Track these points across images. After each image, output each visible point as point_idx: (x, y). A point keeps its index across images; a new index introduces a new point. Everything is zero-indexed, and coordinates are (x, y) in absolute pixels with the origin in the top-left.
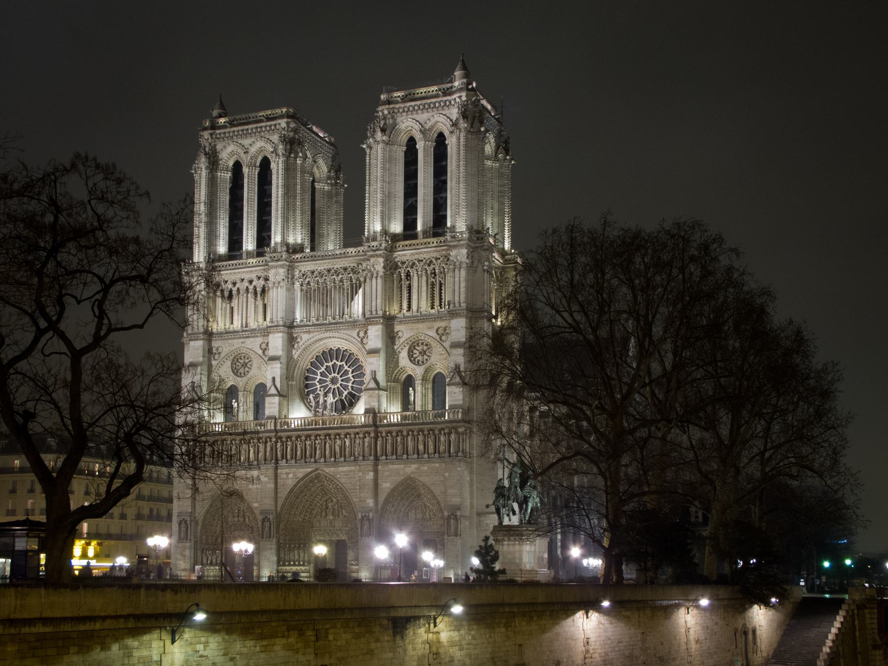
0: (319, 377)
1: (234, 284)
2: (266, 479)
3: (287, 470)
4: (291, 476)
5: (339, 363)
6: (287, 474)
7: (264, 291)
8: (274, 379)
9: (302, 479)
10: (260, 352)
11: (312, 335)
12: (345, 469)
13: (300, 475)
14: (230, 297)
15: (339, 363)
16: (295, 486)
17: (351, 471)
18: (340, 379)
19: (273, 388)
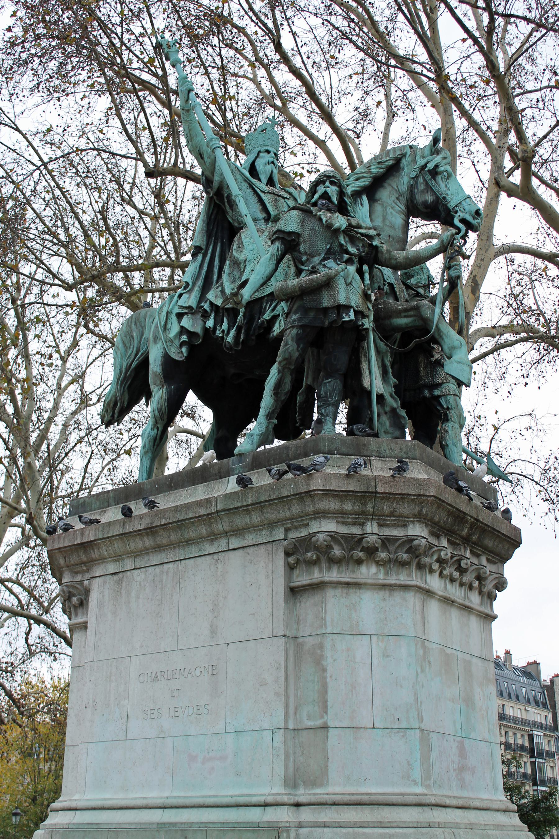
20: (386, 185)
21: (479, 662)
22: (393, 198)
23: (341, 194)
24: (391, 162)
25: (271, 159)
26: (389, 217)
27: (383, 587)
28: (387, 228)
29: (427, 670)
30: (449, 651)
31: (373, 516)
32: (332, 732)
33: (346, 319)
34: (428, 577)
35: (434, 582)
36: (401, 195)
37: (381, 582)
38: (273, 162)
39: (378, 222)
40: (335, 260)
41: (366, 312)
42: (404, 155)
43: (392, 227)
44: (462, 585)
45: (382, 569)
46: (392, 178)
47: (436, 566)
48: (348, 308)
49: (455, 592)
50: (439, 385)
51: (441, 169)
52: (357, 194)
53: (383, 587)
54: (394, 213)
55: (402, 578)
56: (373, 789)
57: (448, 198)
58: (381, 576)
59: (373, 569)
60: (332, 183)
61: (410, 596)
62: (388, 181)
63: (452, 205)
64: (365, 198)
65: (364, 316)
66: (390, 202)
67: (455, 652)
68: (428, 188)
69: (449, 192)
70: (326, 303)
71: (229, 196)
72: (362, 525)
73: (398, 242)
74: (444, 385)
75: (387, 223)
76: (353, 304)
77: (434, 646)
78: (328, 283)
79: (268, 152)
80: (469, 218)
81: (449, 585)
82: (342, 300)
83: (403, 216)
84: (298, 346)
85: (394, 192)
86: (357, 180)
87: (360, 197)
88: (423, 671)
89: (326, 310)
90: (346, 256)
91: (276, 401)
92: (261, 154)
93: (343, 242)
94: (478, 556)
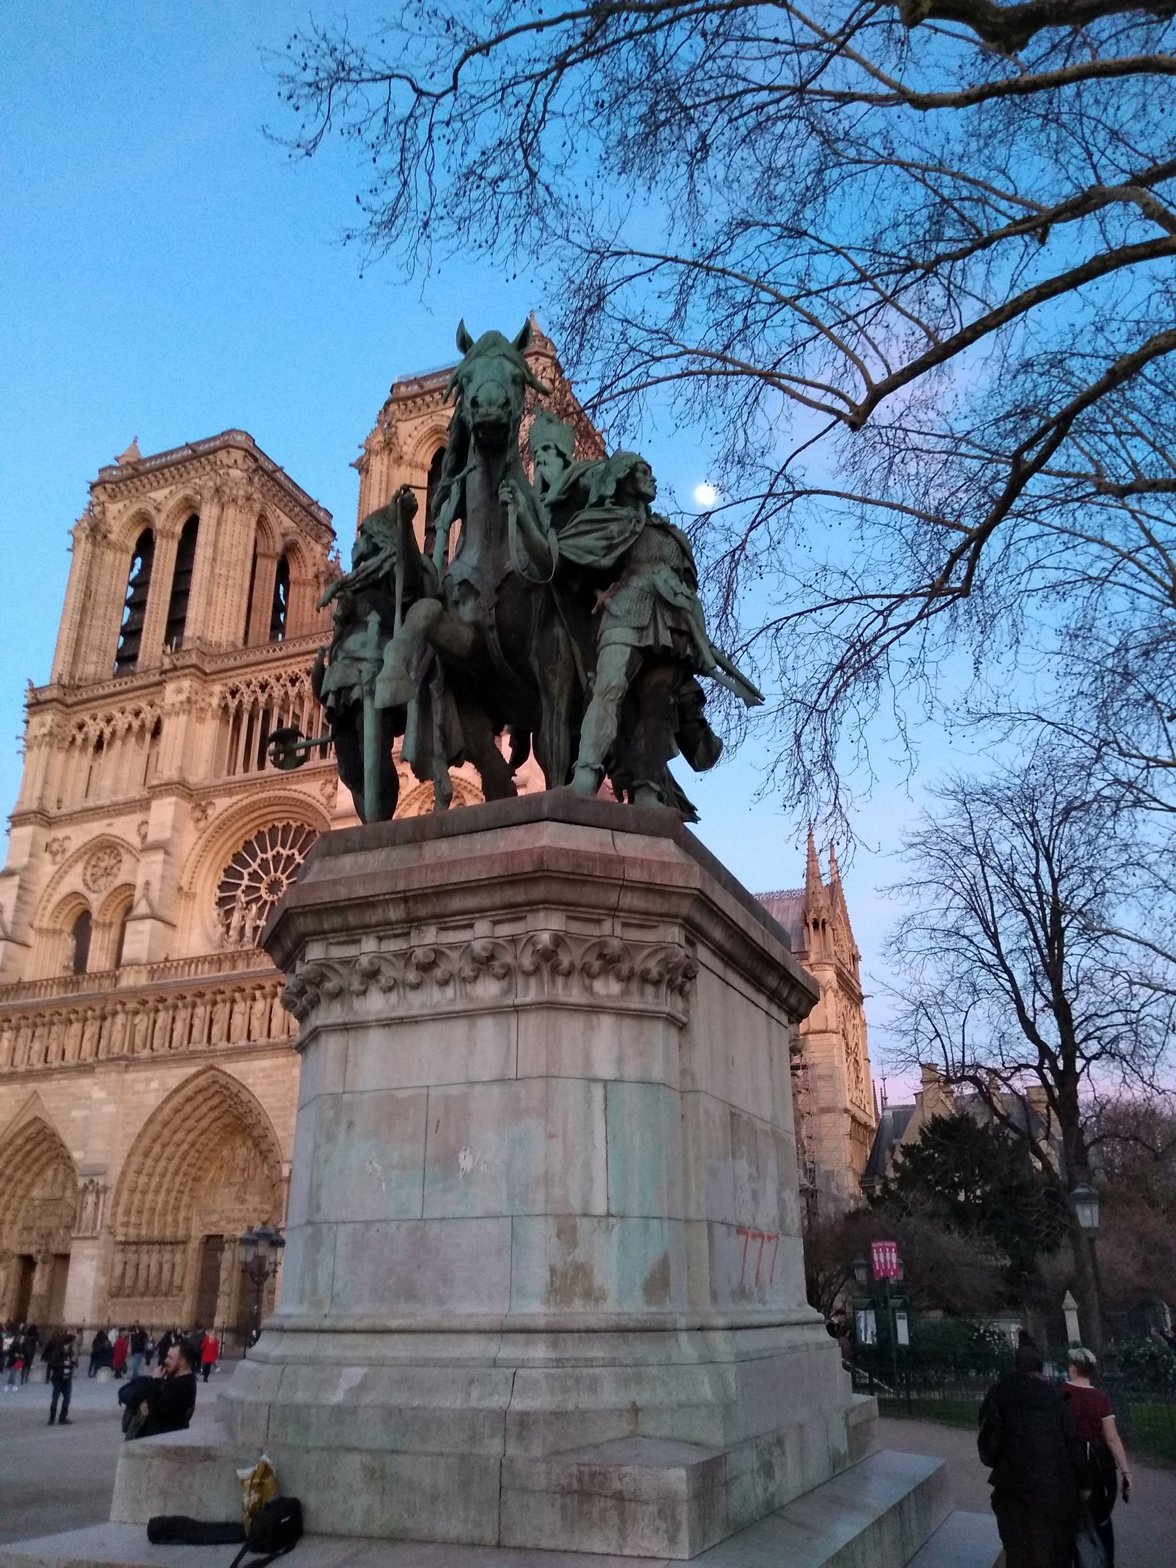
0: (245, 882)
1: (109, 721)
2: (103, 1094)
3: (149, 1074)
4: (154, 1085)
5: (285, 852)
6: (148, 1080)
7: (157, 731)
8: (147, 883)
9: (177, 1090)
10: (136, 841)
11: (235, 798)
12: (266, 1063)
13: (173, 1083)
14: (99, 746)
15: (285, 852)
16: (160, 1109)
17: (277, 1068)
18: (283, 877)
19: (143, 903)
21: (496, 1090)
29: (341, 1136)
30: (399, 1094)
34: (357, 1003)
35: (375, 1004)
41: (354, 680)
44: (444, 983)
65: (351, 688)
67: (424, 1091)
77: (366, 1096)
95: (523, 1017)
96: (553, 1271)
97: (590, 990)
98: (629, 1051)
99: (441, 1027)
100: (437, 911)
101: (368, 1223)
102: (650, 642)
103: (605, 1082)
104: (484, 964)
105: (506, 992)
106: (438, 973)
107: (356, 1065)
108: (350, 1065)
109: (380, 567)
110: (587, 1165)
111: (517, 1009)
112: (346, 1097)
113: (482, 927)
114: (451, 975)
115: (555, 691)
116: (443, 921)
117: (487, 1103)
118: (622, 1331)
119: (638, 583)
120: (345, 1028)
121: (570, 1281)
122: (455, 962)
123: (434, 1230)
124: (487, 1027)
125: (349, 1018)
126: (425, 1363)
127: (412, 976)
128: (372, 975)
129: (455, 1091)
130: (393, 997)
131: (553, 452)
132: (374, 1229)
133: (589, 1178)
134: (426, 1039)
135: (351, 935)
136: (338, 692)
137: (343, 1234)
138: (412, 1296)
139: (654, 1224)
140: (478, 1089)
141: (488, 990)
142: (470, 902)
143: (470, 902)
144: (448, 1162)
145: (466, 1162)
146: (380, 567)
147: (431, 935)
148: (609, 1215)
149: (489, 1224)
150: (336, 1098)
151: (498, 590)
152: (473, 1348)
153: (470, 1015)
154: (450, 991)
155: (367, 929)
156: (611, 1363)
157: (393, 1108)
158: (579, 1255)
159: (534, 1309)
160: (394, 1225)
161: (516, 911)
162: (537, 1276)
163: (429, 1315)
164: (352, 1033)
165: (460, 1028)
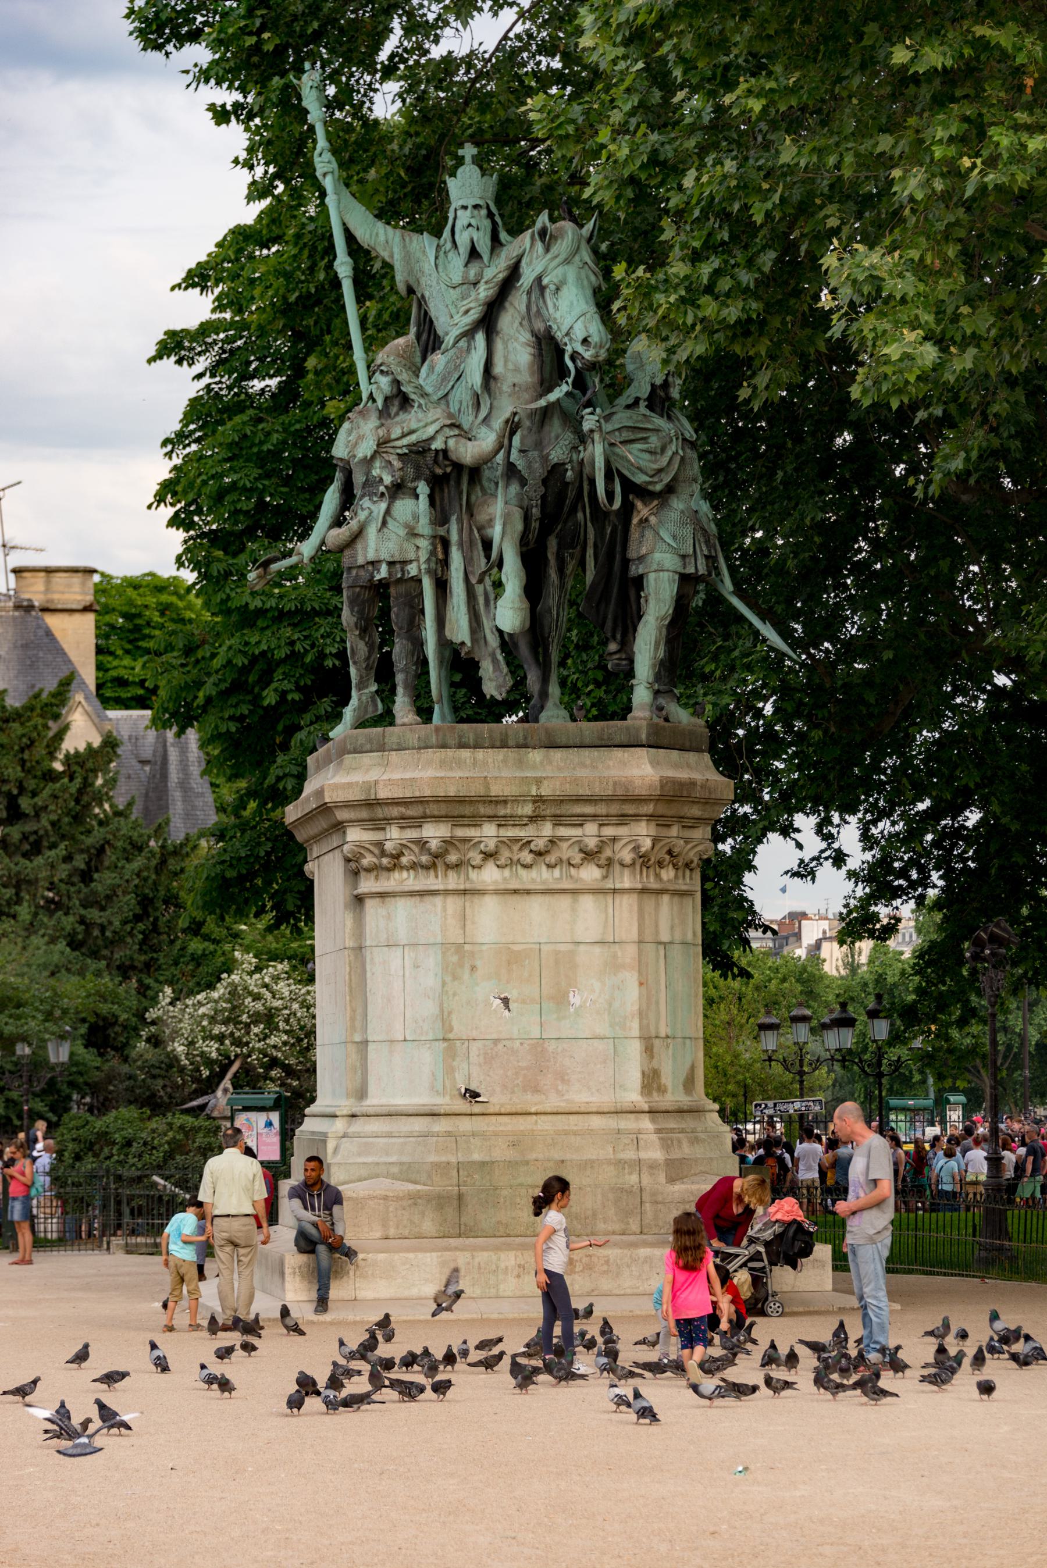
20: (507, 304)
21: (597, 950)
22: (516, 324)
23: (397, 383)
24: (501, 276)
25: (466, 223)
26: (512, 357)
27: (412, 894)
28: (509, 374)
29: (466, 974)
30: (516, 948)
31: (388, 820)
32: (371, 1047)
33: (377, 577)
34: (473, 874)
35: (490, 875)
36: (523, 319)
37: (406, 889)
38: (470, 225)
39: (498, 369)
40: (371, 495)
41: (412, 556)
42: (523, 255)
43: (517, 370)
45: (412, 872)
46: (513, 292)
47: (477, 858)
48: (379, 562)
49: (541, 876)
50: (641, 559)
51: (545, 281)
52: (469, 334)
53: (412, 894)
54: (519, 347)
55: (430, 881)
56: (401, 1101)
57: (555, 327)
58: (411, 881)
59: (405, 874)
60: (382, 372)
61: (438, 900)
62: (510, 298)
63: (559, 335)
64: (480, 338)
66: (512, 332)
68: (539, 313)
69: (558, 315)
70: (361, 561)
71: (423, 296)
72: (384, 829)
73: (526, 390)
74: (649, 558)
75: (511, 366)
76: (384, 555)
77: (484, 947)
78: (358, 535)
79: (465, 208)
80: (580, 349)
81: (522, 872)
82: (371, 556)
83: (530, 350)
84: (352, 611)
85: (516, 315)
86: (467, 312)
87: (473, 338)
88: (455, 978)
89: (363, 566)
90: (382, 489)
91: (358, 670)
92: (460, 213)
93: (375, 472)
94: (581, 825)
95: (618, 897)
96: (643, 1073)
97: (657, 876)
98: (676, 921)
99: (547, 899)
100: (558, 812)
101: (496, 1041)
102: (693, 571)
103: (665, 944)
104: (589, 855)
105: (605, 877)
106: (551, 858)
107: (473, 923)
108: (468, 923)
109: (432, 438)
110: (657, 1003)
111: (615, 891)
112: (467, 947)
113: (591, 828)
114: (561, 860)
115: (568, 572)
116: (558, 820)
117: (591, 957)
118: (680, 1111)
119: (678, 504)
120: (465, 892)
121: (651, 1081)
122: (565, 851)
123: (551, 1047)
124: (587, 902)
125: (468, 886)
126: (566, 1133)
127: (527, 857)
128: (488, 856)
129: (563, 948)
130: (507, 872)
131: (484, 212)
132: (500, 1046)
133: (658, 1013)
134: (536, 906)
135: (475, 820)
136: (391, 564)
137: (475, 1047)
138: (536, 1090)
139: (688, 1041)
140: (582, 947)
141: (590, 874)
142: (589, 809)
143: (589, 809)
144: (561, 999)
145: (575, 999)
146: (432, 438)
147: (547, 829)
148: (667, 1037)
149: (596, 1042)
150: (459, 948)
151: (545, 482)
152: (596, 1122)
153: (574, 892)
154: (557, 872)
155: (491, 818)
156: (682, 1131)
157: (512, 958)
158: (655, 1064)
159: (633, 1096)
160: (518, 1042)
161: (623, 819)
162: (634, 1076)
163: (553, 1102)
164: (468, 897)
165: (565, 901)
